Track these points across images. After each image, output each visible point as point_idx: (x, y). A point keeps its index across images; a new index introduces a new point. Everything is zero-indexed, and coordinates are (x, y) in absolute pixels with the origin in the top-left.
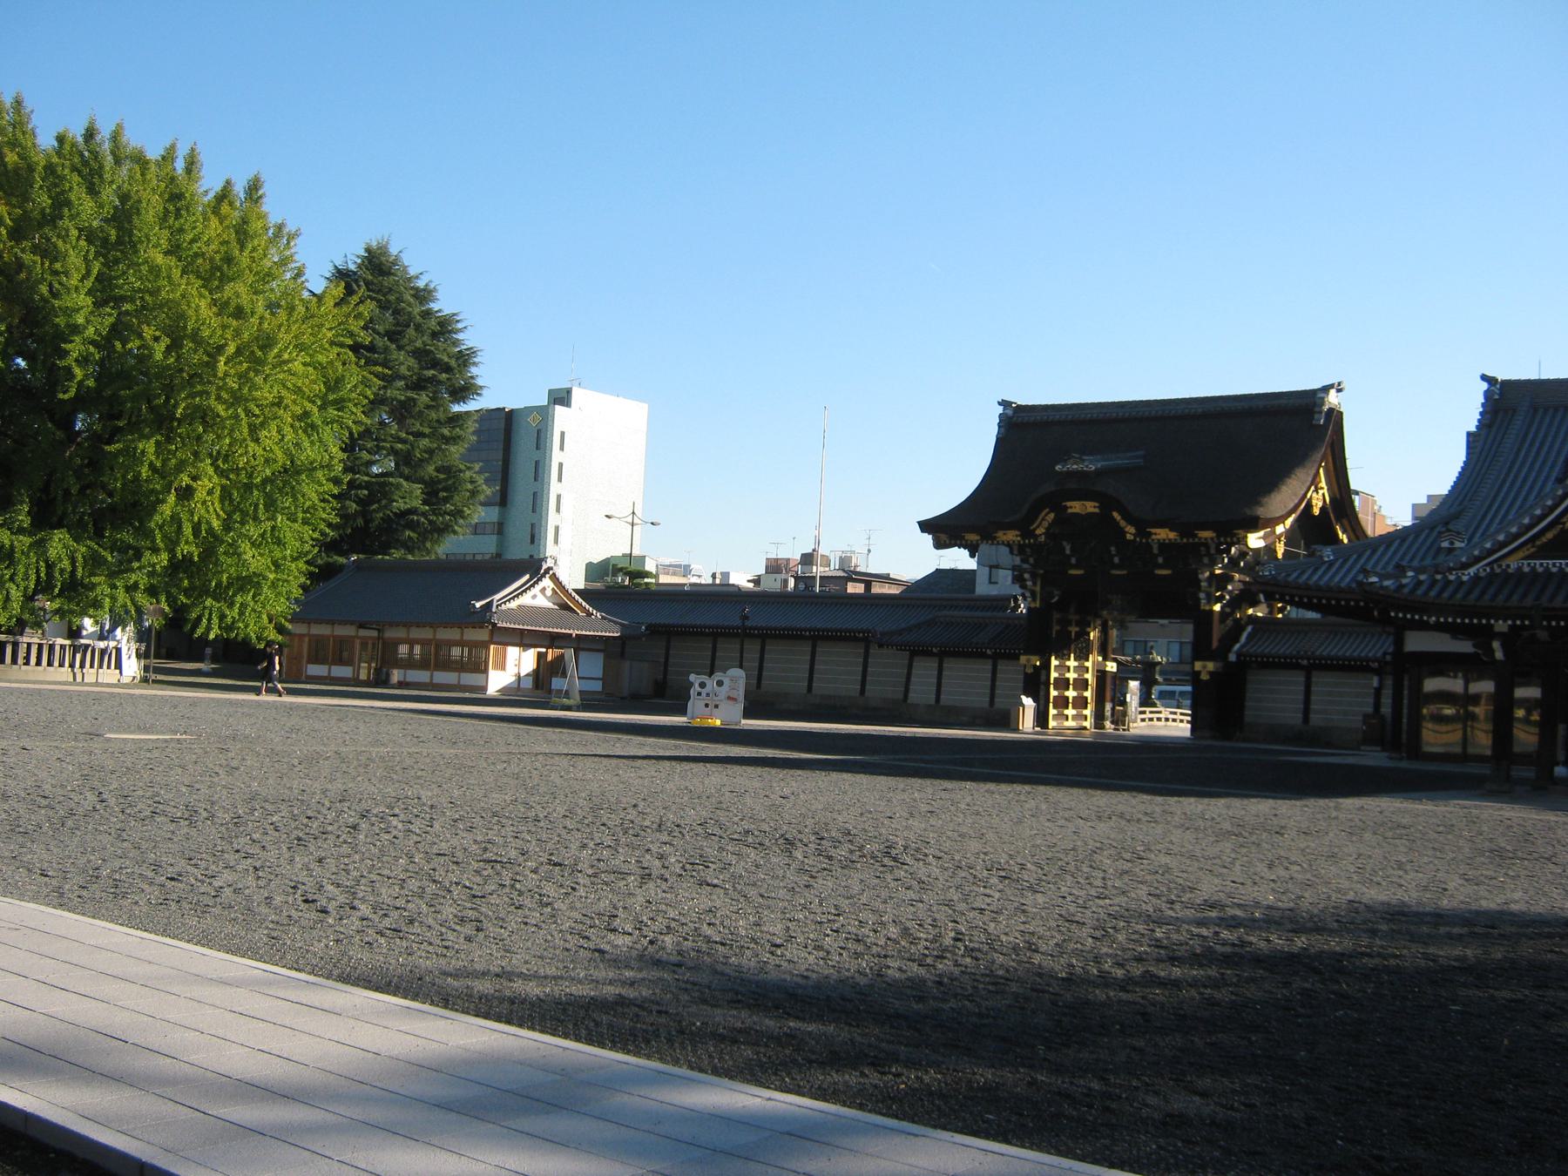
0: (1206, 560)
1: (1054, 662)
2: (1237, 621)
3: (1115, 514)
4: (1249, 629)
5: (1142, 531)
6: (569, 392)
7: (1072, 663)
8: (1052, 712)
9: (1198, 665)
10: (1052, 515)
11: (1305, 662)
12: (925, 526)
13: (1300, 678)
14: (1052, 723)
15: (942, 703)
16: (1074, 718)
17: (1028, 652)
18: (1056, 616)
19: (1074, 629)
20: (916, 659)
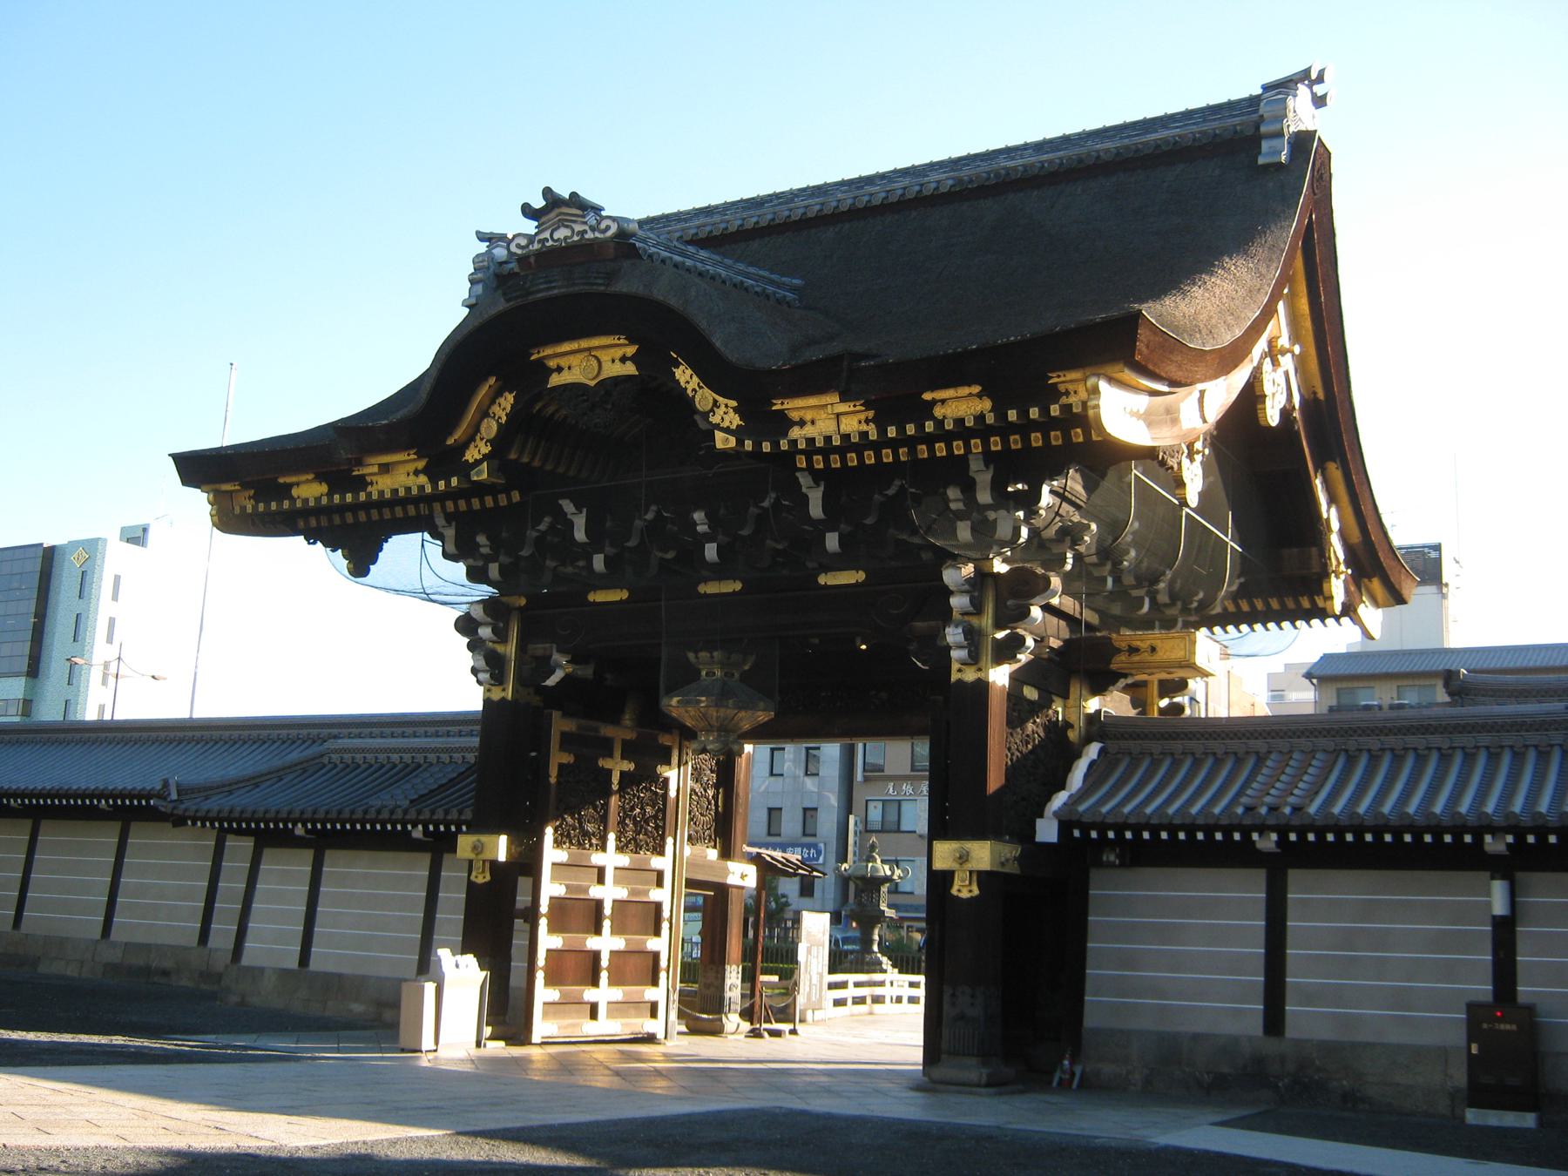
0: (964, 532)
1: (552, 854)
2: (1057, 730)
3: (684, 375)
4: (1093, 751)
5: (762, 419)
6: (145, 530)
7: (611, 858)
8: (544, 994)
9: (945, 853)
10: (508, 400)
11: (1267, 842)
12: (196, 468)
13: (1245, 892)
14: (542, 1027)
15: (315, 965)
16: (617, 1008)
17: (486, 824)
18: (560, 724)
19: (618, 766)
20: (268, 853)
